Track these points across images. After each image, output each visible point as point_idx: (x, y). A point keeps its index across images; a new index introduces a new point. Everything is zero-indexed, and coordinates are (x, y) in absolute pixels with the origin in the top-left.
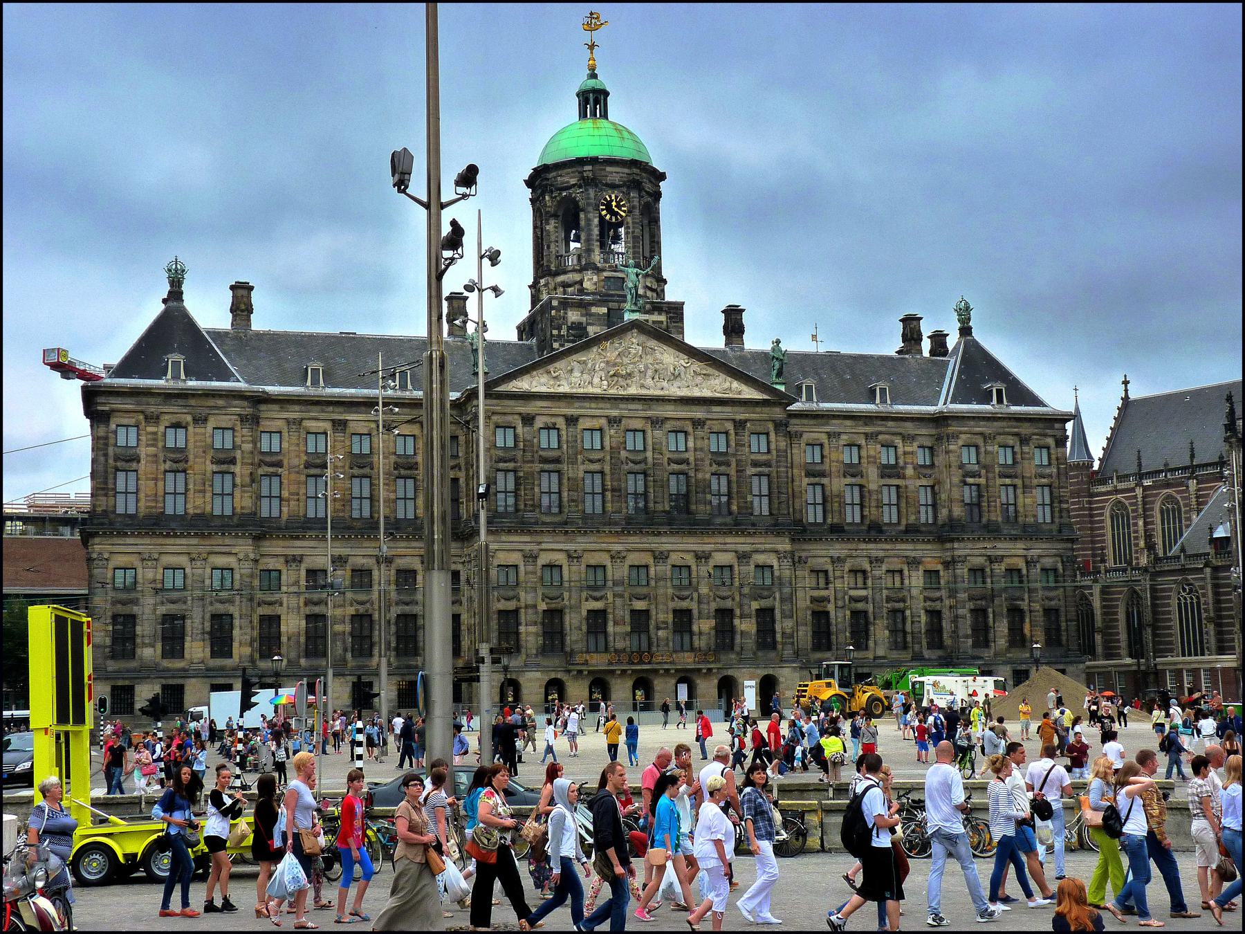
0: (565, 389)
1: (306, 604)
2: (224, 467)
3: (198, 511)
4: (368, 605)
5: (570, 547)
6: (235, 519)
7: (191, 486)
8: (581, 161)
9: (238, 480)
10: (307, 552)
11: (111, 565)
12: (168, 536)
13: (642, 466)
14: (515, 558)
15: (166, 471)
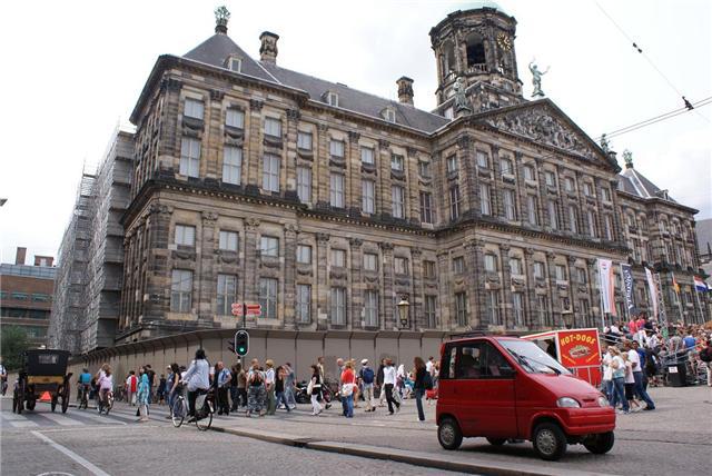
0: (515, 132)
1: (331, 277)
2: (273, 150)
3: (252, 183)
4: (375, 283)
5: (528, 246)
6: (282, 196)
7: (246, 161)
8: (485, 10)
9: (284, 162)
10: (333, 233)
11: (173, 222)
12: (227, 200)
13: (554, 196)
14: (495, 249)
15: (226, 144)
